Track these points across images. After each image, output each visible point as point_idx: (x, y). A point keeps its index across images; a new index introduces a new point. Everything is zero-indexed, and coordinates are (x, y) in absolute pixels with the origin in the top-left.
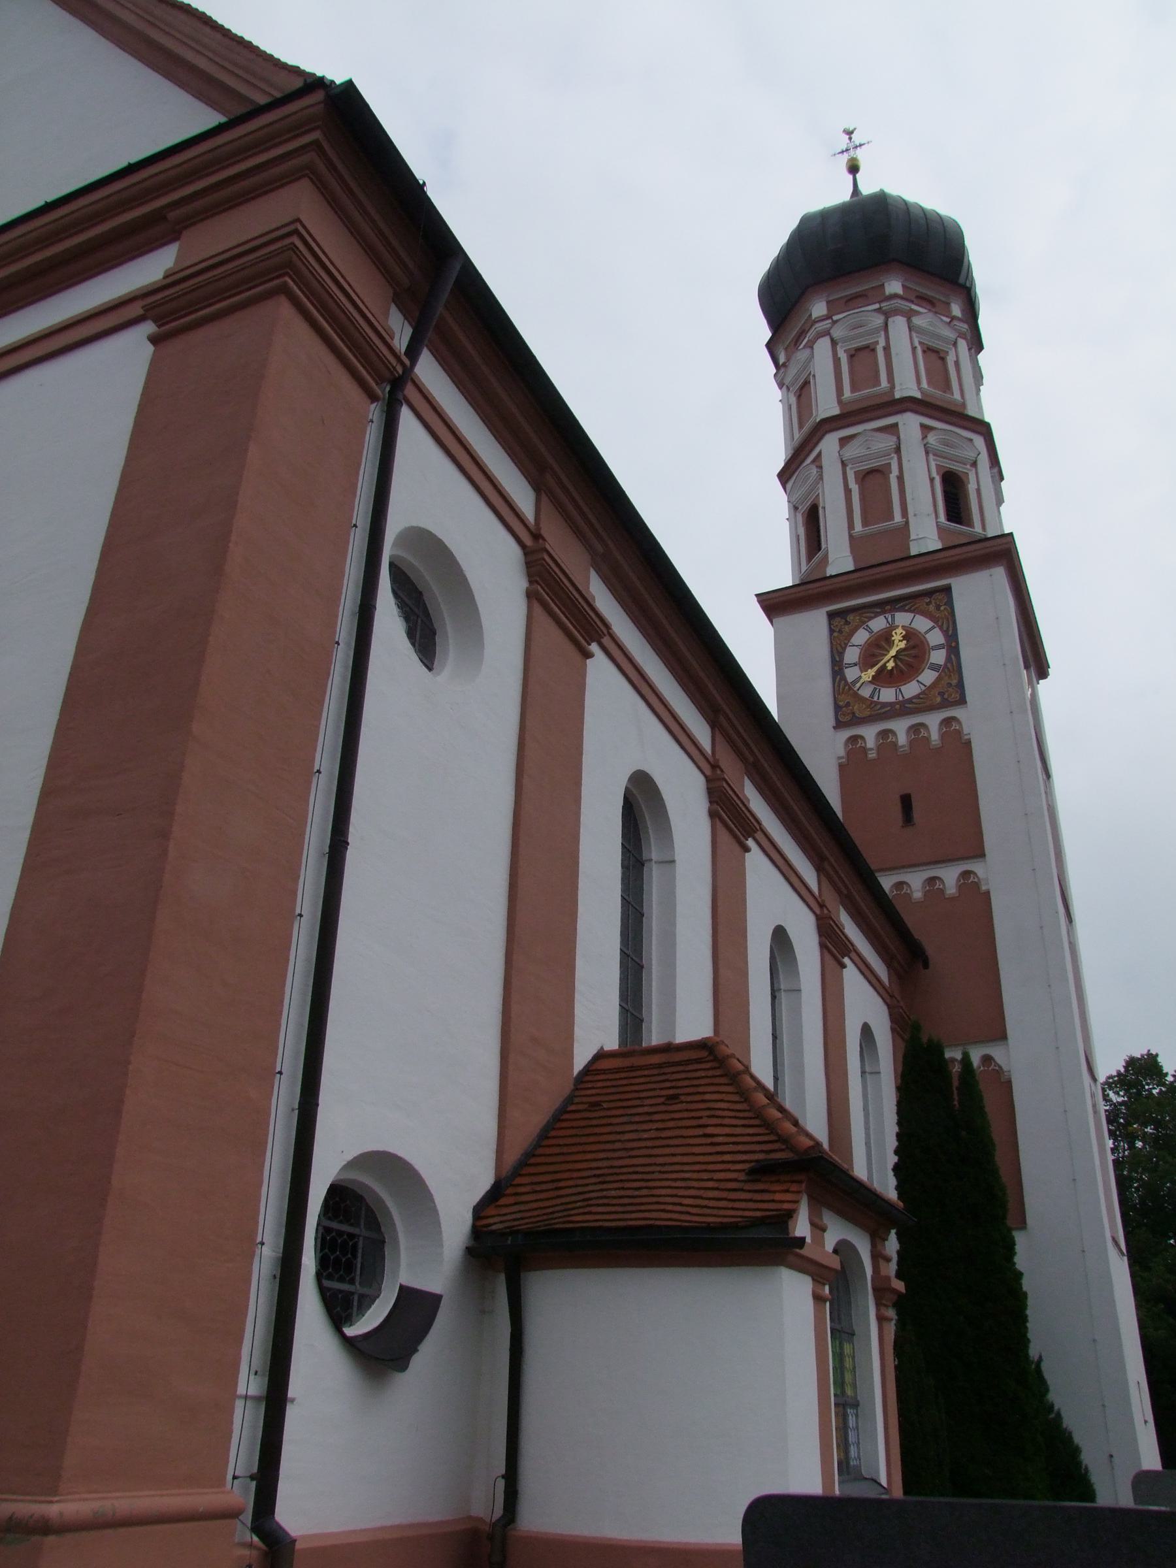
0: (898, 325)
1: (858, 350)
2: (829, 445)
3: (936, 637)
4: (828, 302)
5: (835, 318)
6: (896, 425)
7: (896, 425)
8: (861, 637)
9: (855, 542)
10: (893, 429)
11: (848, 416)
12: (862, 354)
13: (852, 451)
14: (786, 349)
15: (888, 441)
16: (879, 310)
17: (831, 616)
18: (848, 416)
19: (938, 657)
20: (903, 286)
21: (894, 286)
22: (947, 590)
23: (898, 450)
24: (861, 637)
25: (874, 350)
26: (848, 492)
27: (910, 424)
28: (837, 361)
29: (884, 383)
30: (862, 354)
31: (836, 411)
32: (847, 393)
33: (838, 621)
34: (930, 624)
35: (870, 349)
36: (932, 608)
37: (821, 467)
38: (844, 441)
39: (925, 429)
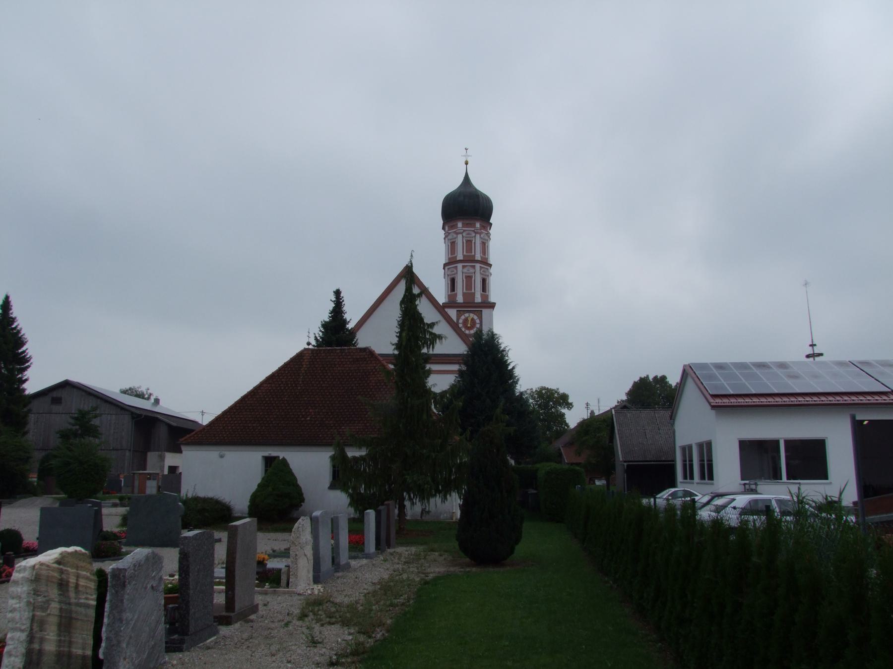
0: (478, 236)
1: (468, 240)
2: (460, 266)
3: (478, 321)
6: (475, 266)
7: (475, 266)
9: (464, 294)
10: (474, 267)
12: (469, 244)
13: (465, 270)
14: (448, 226)
15: (473, 271)
16: (474, 231)
19: (478, 326)
20: (480, 224)
21: (478, 225)
22: (481, 311)
23: (475, 273)
25: (472, 242)
26: (463, 280)
27: (478, 266)
28: (463, 242)
29: (473, 253)
30: (469, 244)
31: (462, 258)
34: (477, 318)
35: (471, 241)
36: (478, 314)
38: (464, 267)
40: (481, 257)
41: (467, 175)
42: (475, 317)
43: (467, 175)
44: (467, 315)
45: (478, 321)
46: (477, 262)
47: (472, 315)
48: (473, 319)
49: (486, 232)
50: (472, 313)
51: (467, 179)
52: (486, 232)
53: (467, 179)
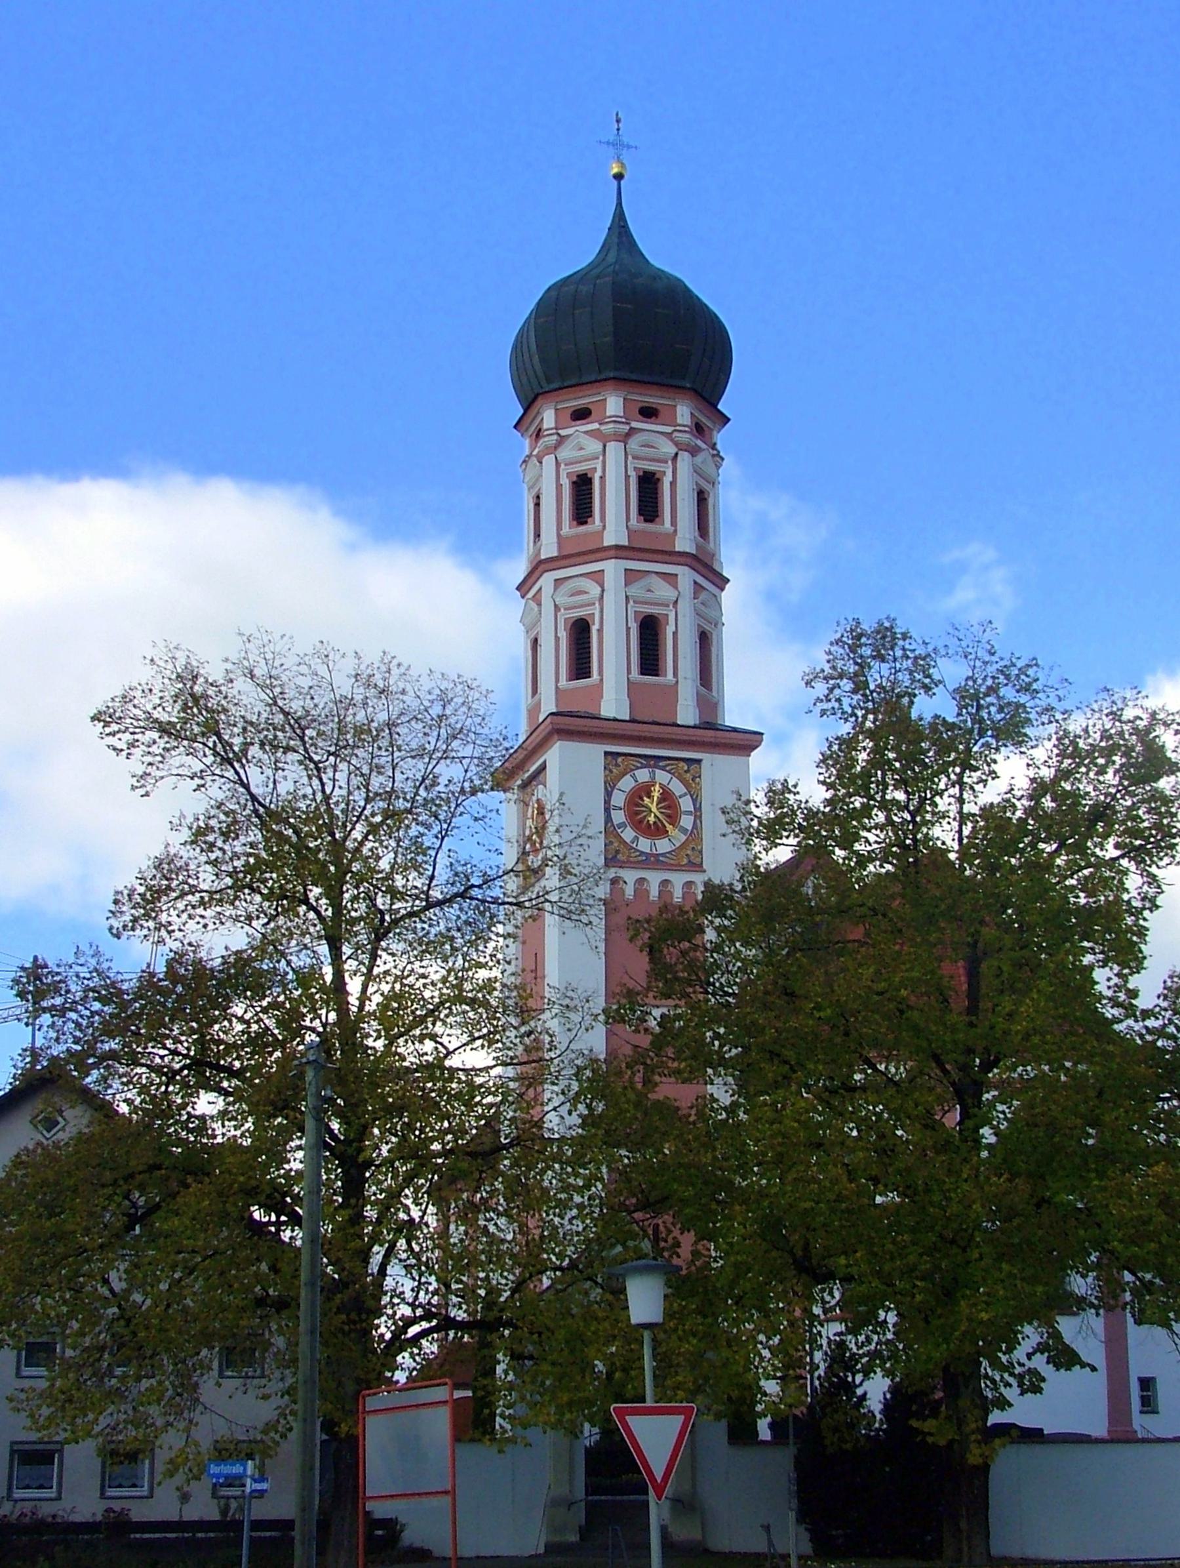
2: (547, 581)
4: (556, 410)
5: (563, 432)
8: (627, 783)
10: (598, 577)
11: (563, 559)
17: (606, 753)
18: (563, 559)
21: (614, 404)
24: (627, 783)
26: (557, 639)
28: (559, 486)
32: (566, 530)
33: (609, 758)
37: (539, 605)
39: (631, 576)
40: (631, 533)
41: (619, 215)
42: (677, 788)
43: (620, 219)
44: (643, 775)
45: (686, 804)
46: (619, 552)
47: (662, 777)
48: (667, 796)
49: (669, 429)
50: (663, 768)
51: (620, 228)
52: (669, 429)
53: (620, 228)
